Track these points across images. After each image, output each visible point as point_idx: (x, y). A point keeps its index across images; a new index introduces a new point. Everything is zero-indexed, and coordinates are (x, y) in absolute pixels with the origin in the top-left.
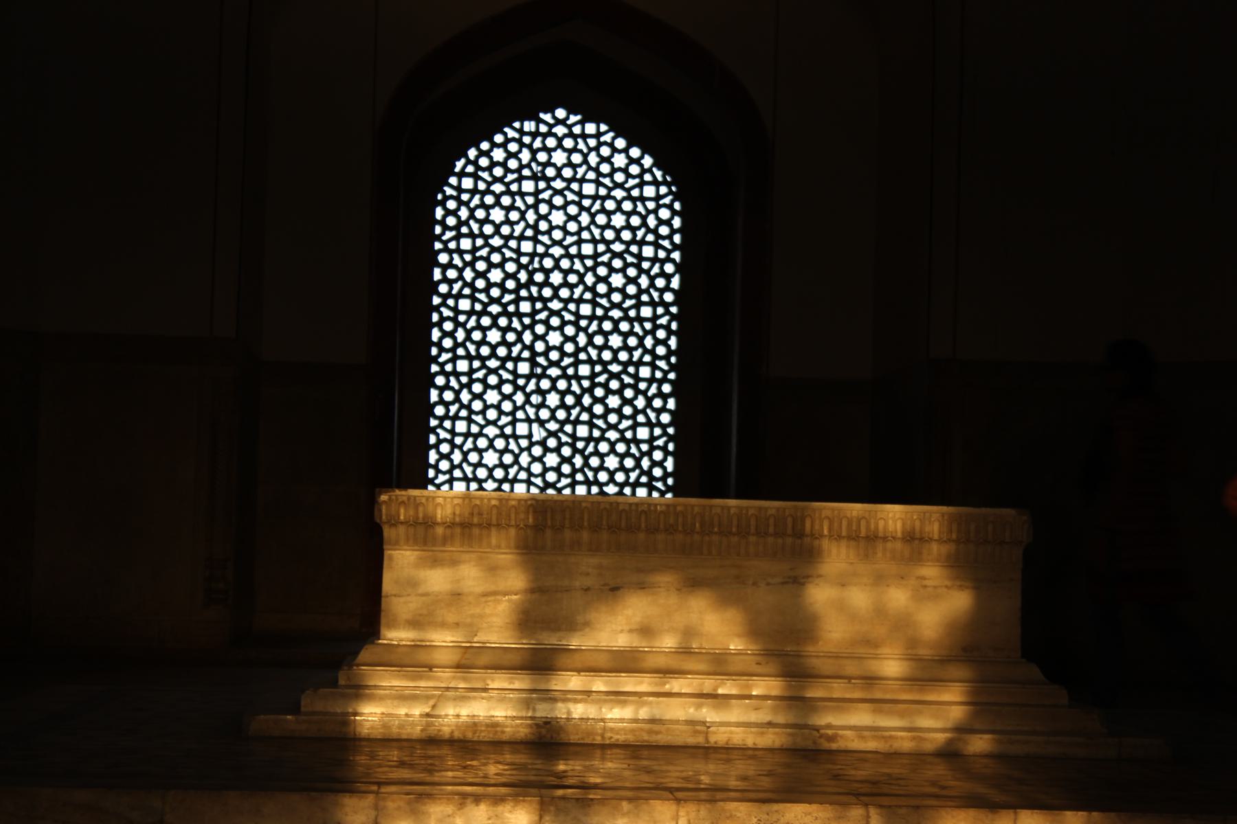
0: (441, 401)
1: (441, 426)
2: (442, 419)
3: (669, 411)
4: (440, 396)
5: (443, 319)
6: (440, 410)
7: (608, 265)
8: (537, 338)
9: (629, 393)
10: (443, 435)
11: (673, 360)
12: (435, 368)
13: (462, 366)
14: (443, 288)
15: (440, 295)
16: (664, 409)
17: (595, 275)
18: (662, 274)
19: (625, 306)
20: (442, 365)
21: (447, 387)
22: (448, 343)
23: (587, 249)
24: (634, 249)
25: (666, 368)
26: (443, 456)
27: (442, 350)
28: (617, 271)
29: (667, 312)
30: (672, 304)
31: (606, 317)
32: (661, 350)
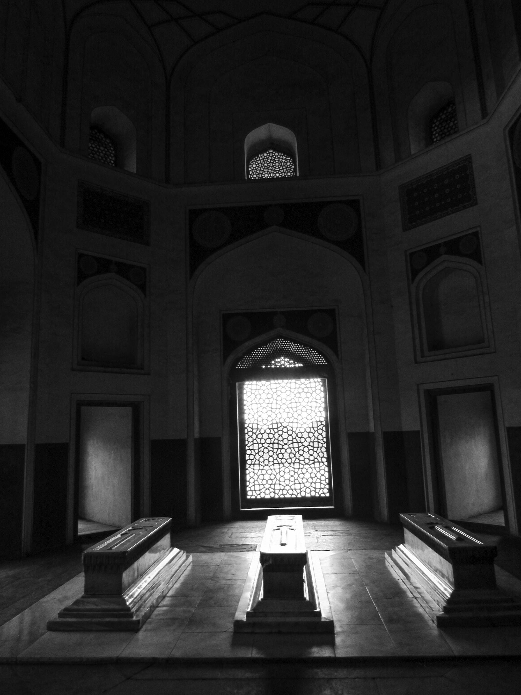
9: (309, 412)
10: (250, 429)
12: (245, 407)
26: (251, 437)
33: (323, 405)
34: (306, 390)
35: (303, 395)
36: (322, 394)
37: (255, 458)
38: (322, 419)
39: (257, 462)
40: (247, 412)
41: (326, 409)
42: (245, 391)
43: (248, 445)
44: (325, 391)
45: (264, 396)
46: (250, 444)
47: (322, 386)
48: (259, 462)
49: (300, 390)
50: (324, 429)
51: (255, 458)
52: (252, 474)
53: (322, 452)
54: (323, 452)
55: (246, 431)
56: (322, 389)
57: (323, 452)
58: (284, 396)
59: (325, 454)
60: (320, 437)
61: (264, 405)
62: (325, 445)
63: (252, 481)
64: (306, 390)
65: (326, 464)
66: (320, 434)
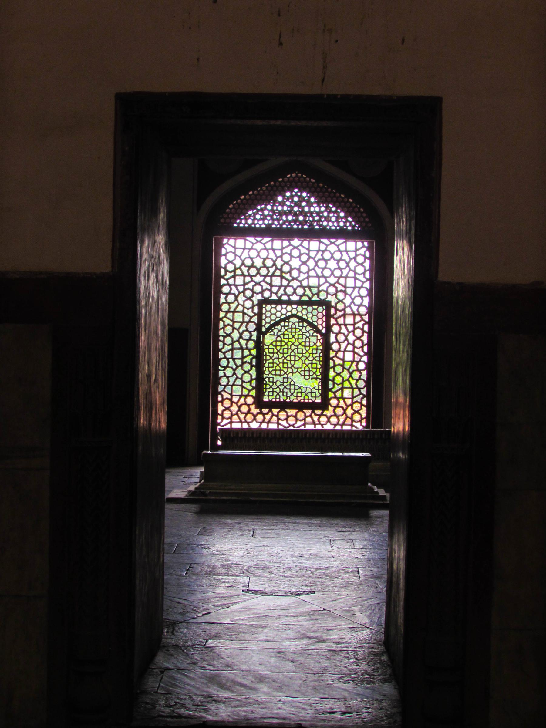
0: (227, 302)
1: (225, 317)
2: (227, 312)
3: (365, 306)
4: (226, 298)
6: (225, 307)
10: (227, 322)
12: (223, 282)
13: (239, 280)
16: (361, 305)
20: (227, 280)
21: (230, 293)
25: (364, 280)
27: (226, 271)
33: (367, 285)
34: (337, 256)
35: (332, 264)
36: (367, 265)
37: (234, 374)
38: (363, 310)
39: (239, 382)
40: (226, 289)
41: (370, 292)
42: (223, 251)
43: (223, 350)
44: (370, 258)
45: (258, 263)
46: (227, 348)
47: (368, 249)
48: (243, 382)
49: (327, 256)
50: (366, 328)
51: (234, 374)
52: (227, 403)
54: (360, 371)
55: (221, 324)
56: (367, 254)
57: (360, 371)
58: (295, 263)
59: (364, 373)
61: (258, 279)
62: (365, 359)
63: (227, 414)
64: (337, 256)
65: (364, 391)
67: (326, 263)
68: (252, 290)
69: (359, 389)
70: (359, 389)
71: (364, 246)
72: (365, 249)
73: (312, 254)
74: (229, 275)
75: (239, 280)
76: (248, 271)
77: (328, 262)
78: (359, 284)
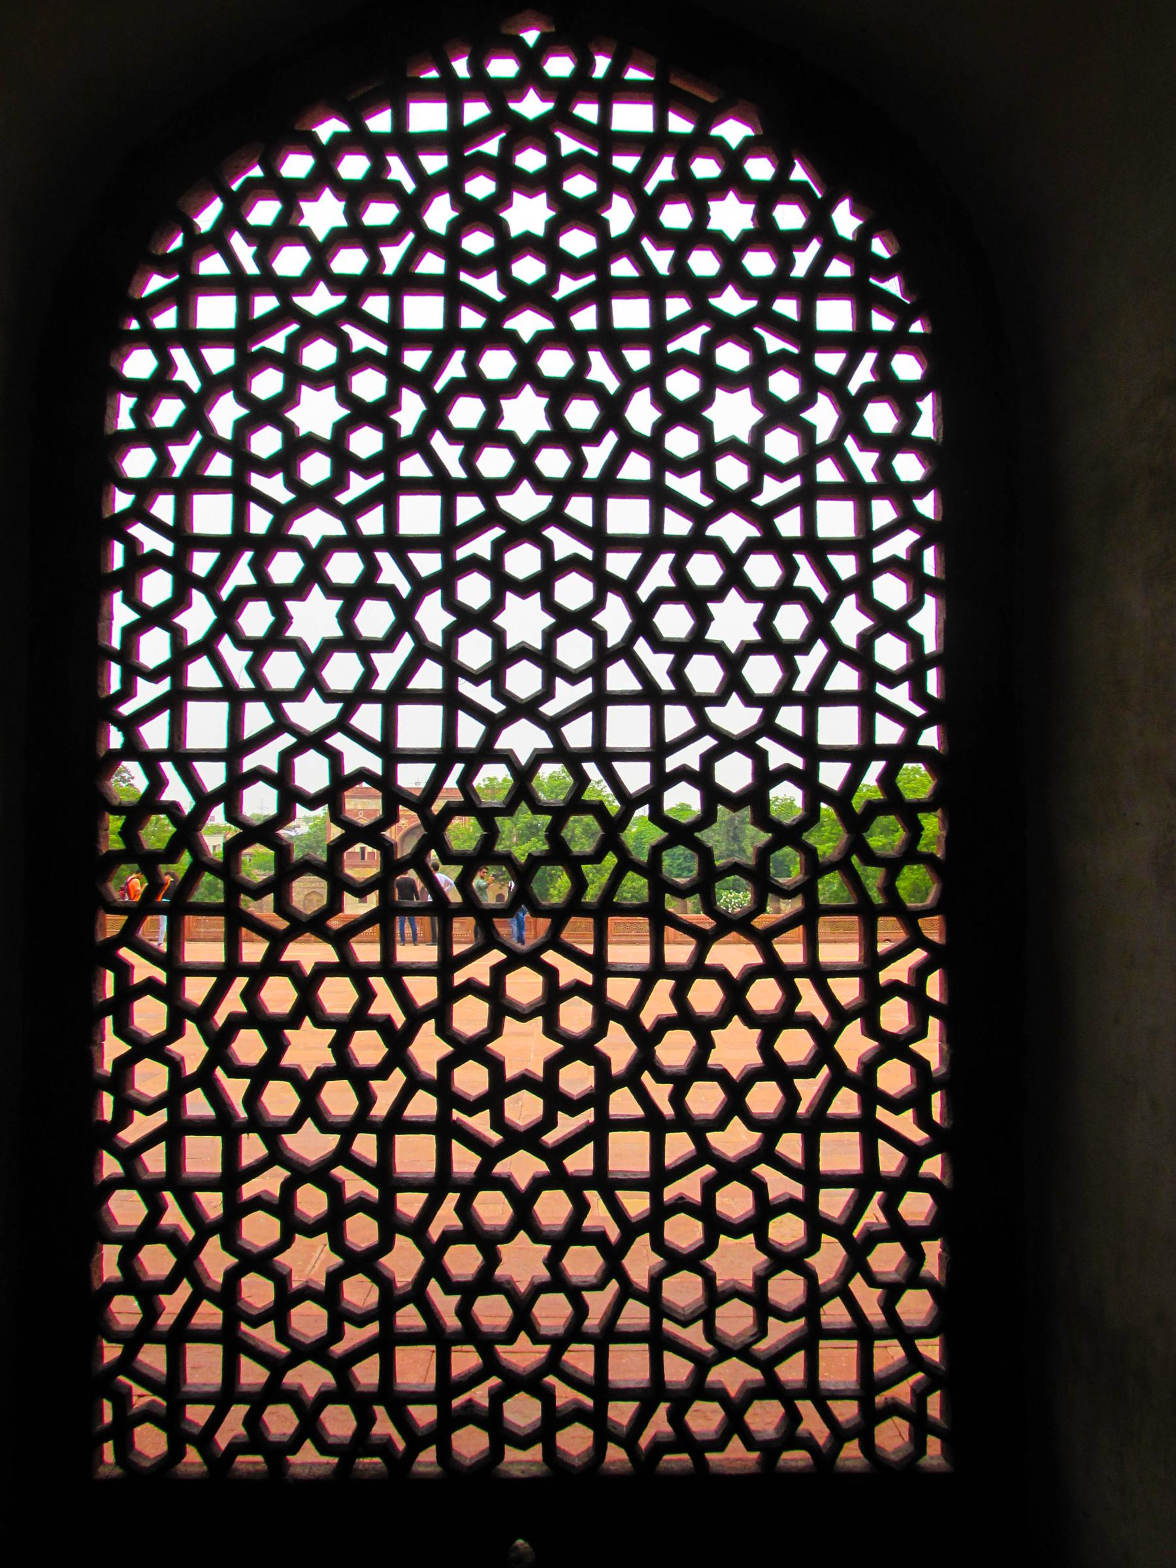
3: (928, 860)
5: (141, 562)
7: (703, 365)
8: (467, 620)
11: (932, 682)
13: (207, 725)
14: (138, 463)
15: (129, 485)
17: (662, 399)
18: (886, 386)
19: (761, 501)
22: (154, 648)
23: (631, 314)
24: (787, 308)
28: (732, 381)
29: (908, 519)
30: (919, 489)
31: (698, 542)
32: (891, 652)
33: (930, 738)
34: (763, 570)
45: (315, 618)
53: (897, 1230)
60: (894, 1077)
66: (894, 1046)
67: (703, 619)
68: (282, 780)
69: (907, 1336)
70: (907, 1336)
71: (908, 519)
72: (909, 537)
73: (620, 564)
74: (147, 692)
75: (207, 725)
76: (254, 669)
77: (713, 607)
78: (888, 732)
